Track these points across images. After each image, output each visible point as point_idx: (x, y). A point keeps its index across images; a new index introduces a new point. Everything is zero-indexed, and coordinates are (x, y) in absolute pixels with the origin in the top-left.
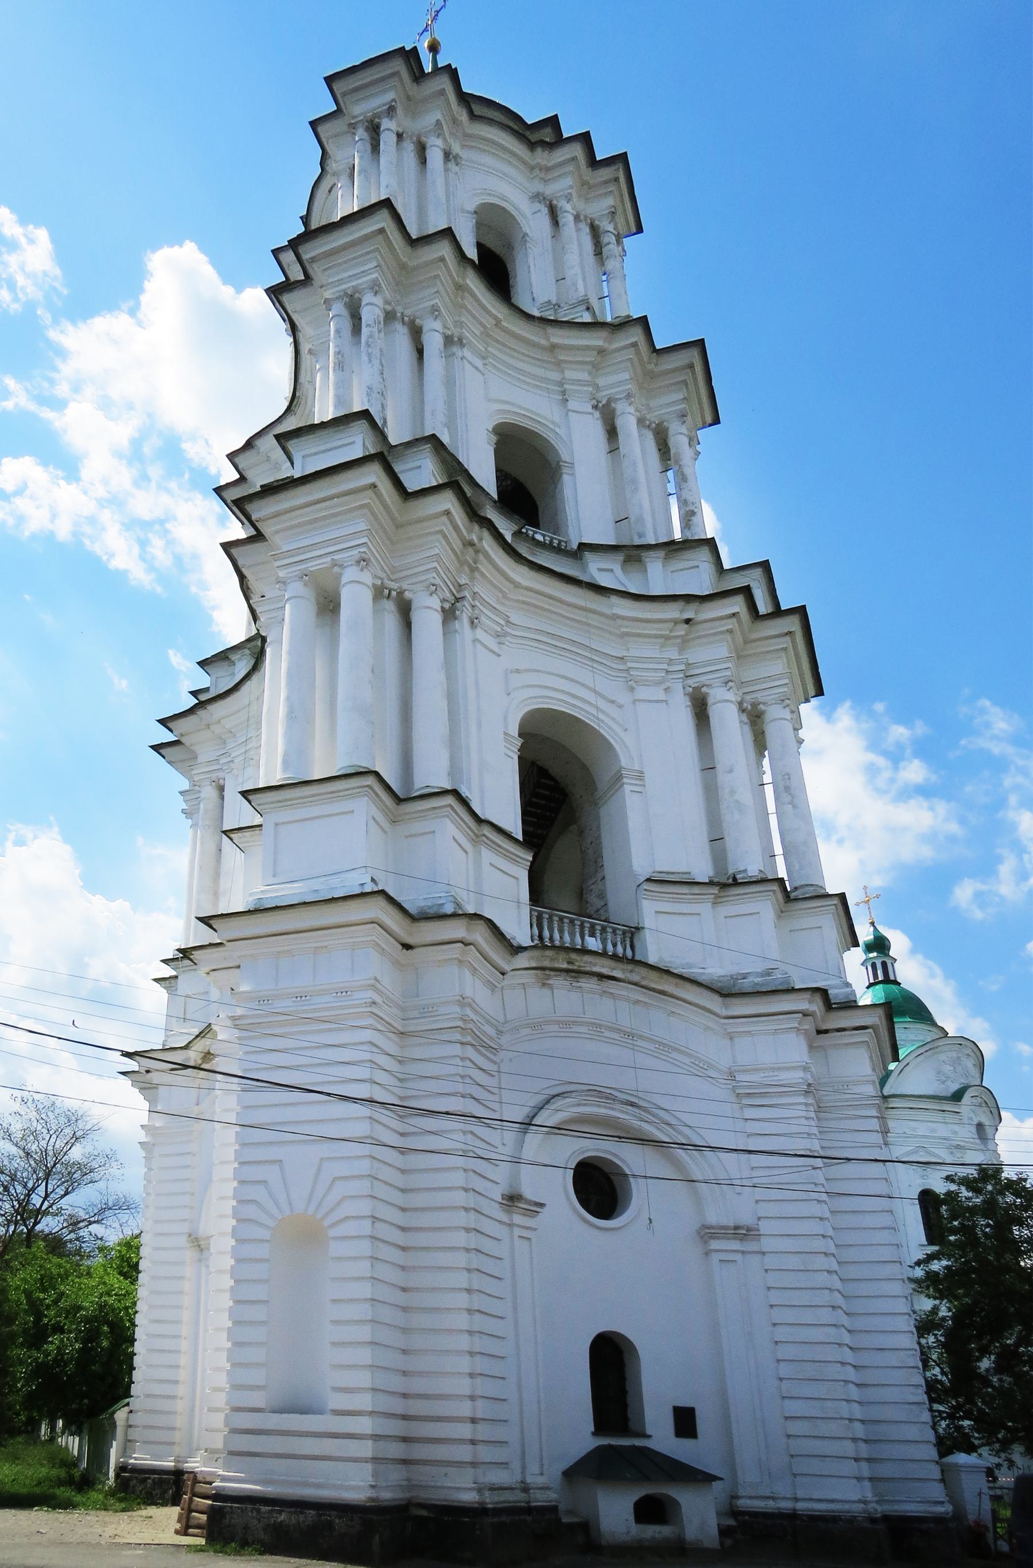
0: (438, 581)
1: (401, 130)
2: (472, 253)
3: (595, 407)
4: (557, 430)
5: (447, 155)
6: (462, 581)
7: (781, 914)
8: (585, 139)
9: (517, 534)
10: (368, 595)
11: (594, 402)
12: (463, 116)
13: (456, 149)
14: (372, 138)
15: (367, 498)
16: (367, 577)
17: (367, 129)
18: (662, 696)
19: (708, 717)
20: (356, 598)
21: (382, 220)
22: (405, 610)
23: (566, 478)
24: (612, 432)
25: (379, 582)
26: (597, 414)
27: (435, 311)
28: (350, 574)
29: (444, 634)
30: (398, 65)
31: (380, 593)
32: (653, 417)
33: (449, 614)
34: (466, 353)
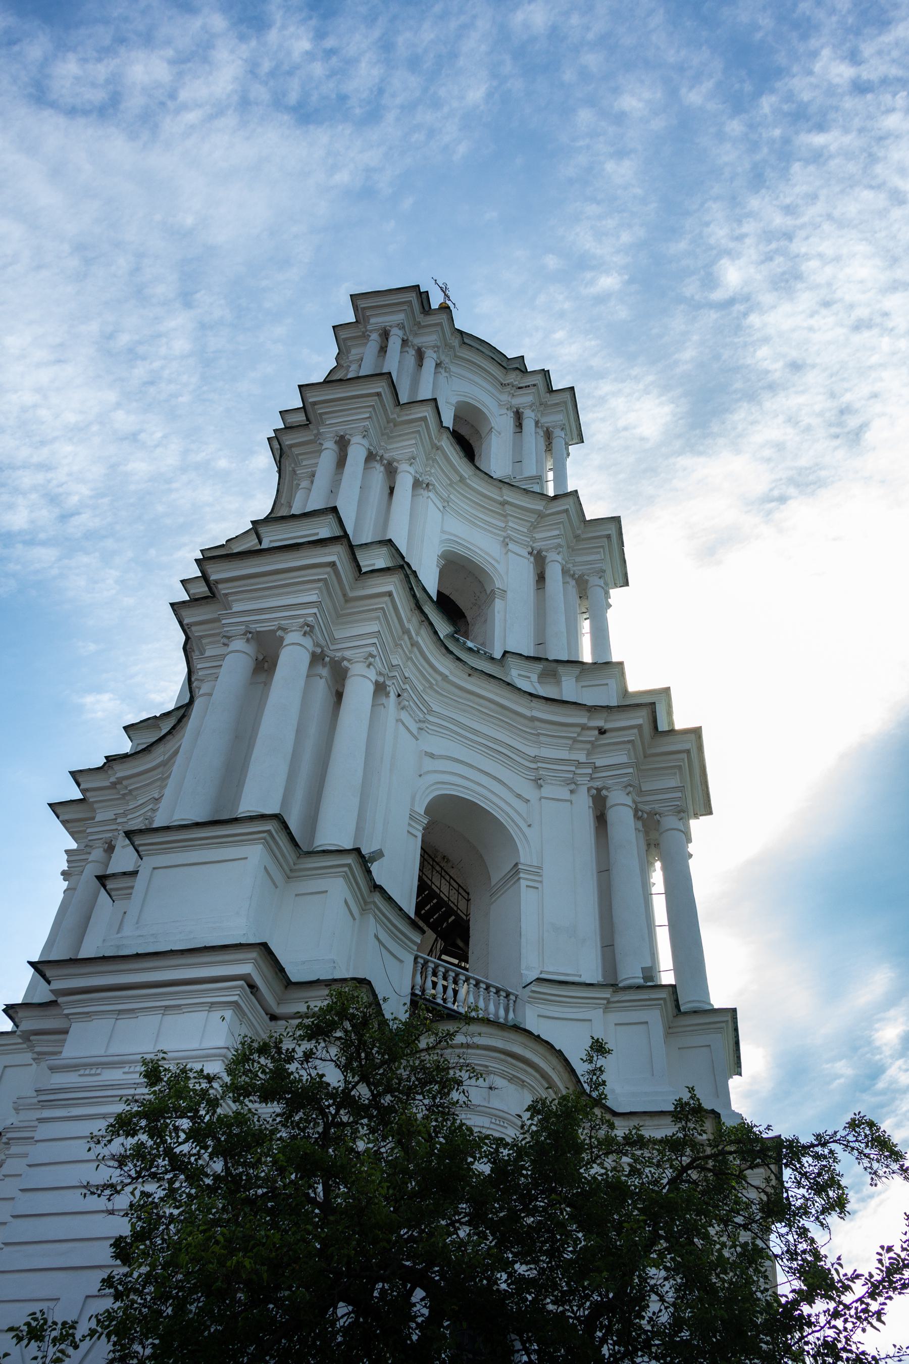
0: (375, 653)
1: (405, 338)
2: (448, 421)
3: (531, 553)
4: (496, 564)
5: (438, 365)
6: (395, 662)
7: (670, 1031)
8: (545, 373)
9: (451, 636)
10: (306, 658)
11: (530, 549)
12: (456, 342)
13: (446, 360)
14: (382, 342)
15: (324, 574)
16: (308, 642)
17: (380, 335)
18: (566, 795)
19: (606, 822)
20: (293, 658)
21: (380, 387)
22: (339, 676)
23: (498, 604)
24: (541, 578)
25: (319, 650)
26: (532, 559)
27: (412, 460)
28: (292, 637)
29: (372, 706)
30: (412, 297)
31: (317, 659)
32: (578, 570)
33: (380, 689)
34: (431, 494)
